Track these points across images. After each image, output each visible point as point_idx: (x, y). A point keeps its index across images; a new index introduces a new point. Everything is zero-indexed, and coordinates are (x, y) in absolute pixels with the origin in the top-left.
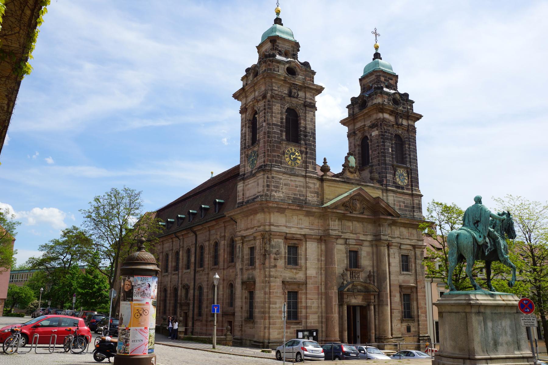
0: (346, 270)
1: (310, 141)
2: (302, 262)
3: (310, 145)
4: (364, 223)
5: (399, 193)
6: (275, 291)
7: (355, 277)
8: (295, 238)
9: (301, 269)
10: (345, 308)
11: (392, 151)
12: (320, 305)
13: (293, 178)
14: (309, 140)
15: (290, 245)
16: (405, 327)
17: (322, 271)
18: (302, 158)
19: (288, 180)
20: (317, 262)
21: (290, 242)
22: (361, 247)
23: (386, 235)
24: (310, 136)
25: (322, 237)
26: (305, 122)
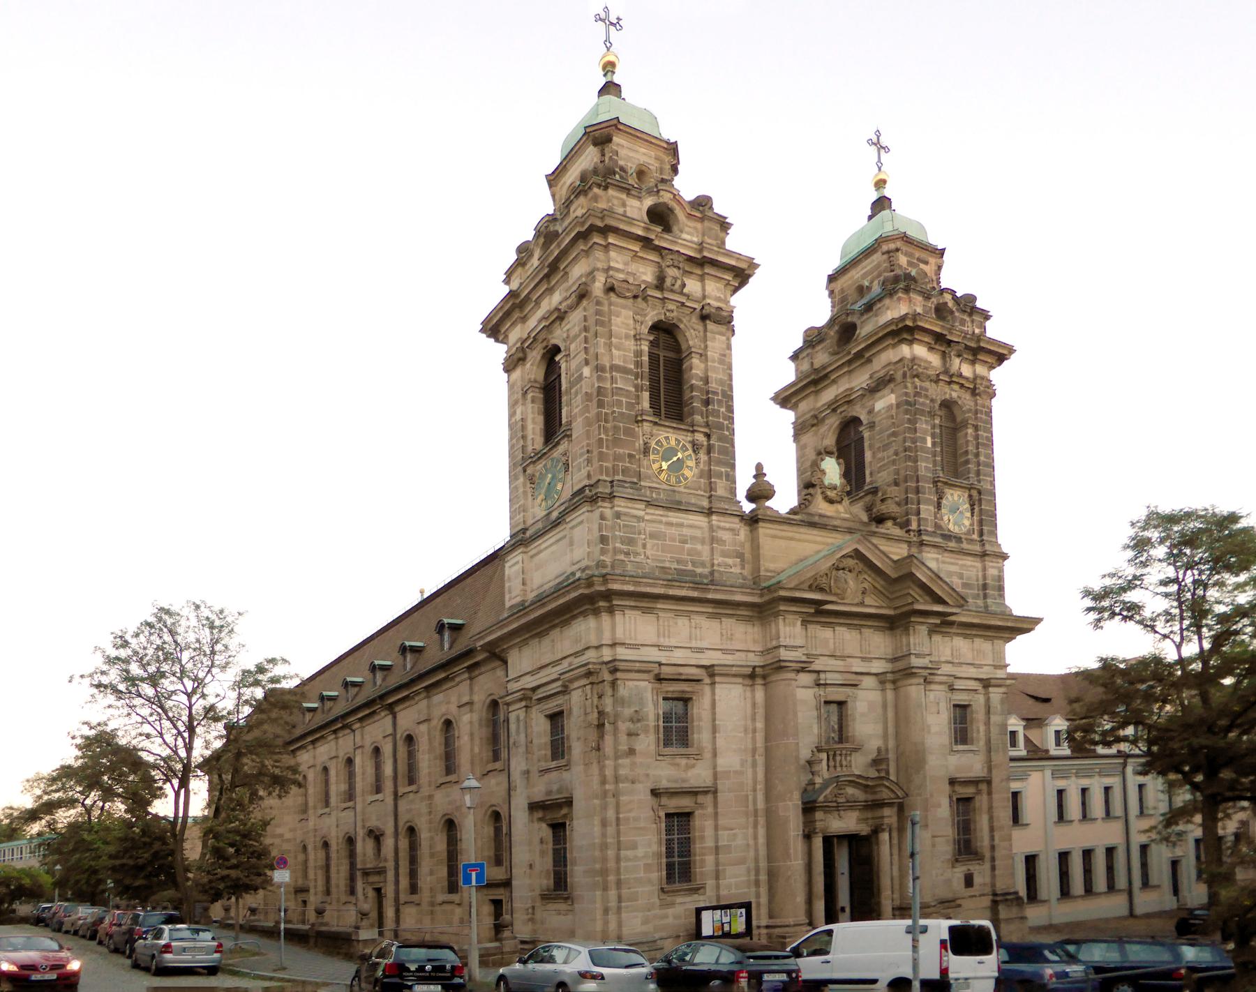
0: (819, 750)
1: (718, 416)
2: (701, 736)
3: (720, 427)
4: (863, 630)
6: (632, 815)
7: (841, 766)
8: (683, 677)
9: (698, 756)
10: (818, 843)
12: (751, 842)
13: (674, 517)
14: (716, 413)
15: (669, 695)
17: (757, 757)
18: (697, 463)
19: (661, 522)
20: (742, 735)
21: (671, 689)
22: (855, 691)
24: (720, 402)
25: (757, 669)
26: (702, 366)
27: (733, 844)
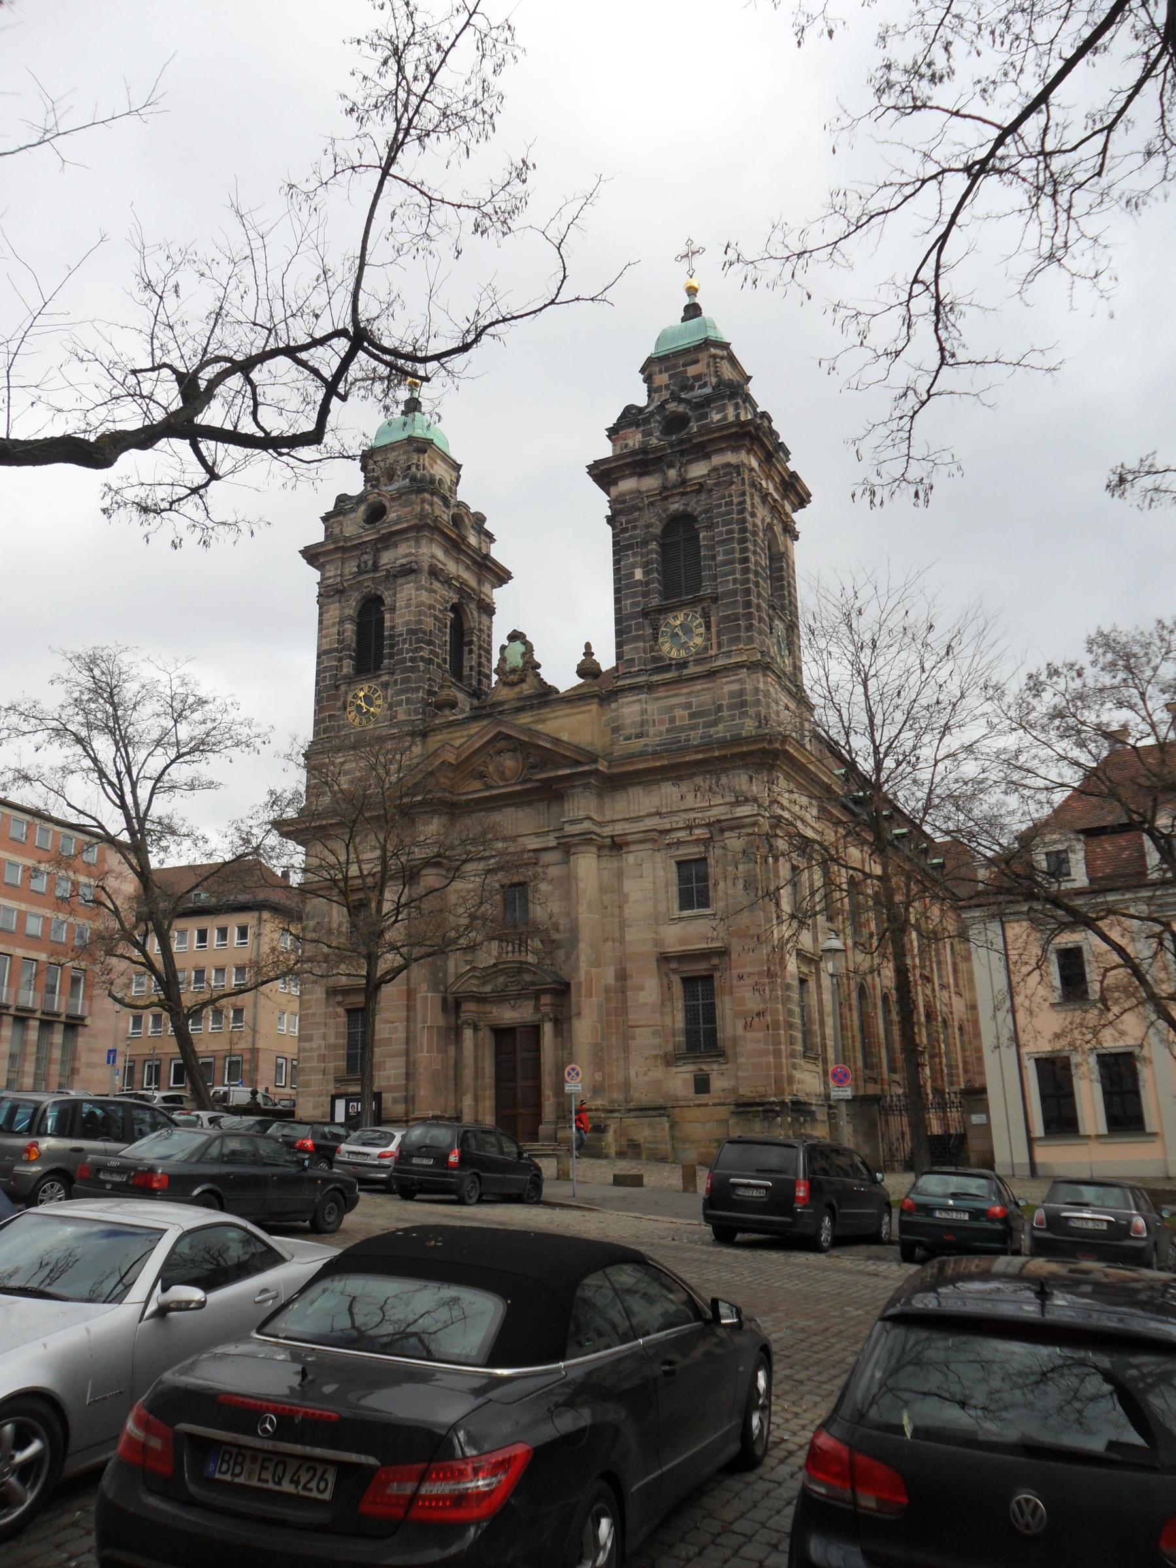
5: (664, 684)
11: (646, 573)
16: (690, 1077)
23: (580, 821)
27: (393, 1036)
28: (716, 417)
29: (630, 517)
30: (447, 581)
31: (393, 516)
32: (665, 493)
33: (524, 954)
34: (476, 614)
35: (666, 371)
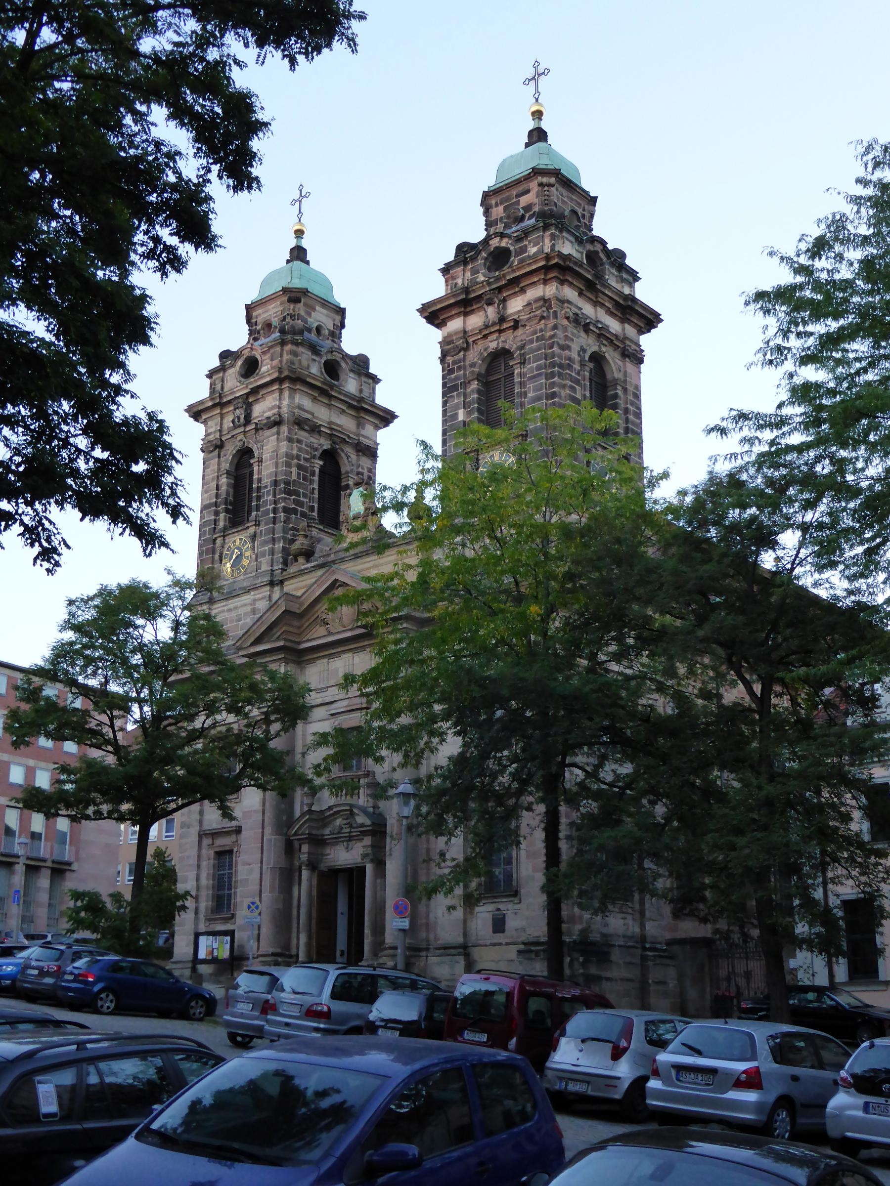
11: (469, 413)
16: (488, 917)
19: (223, 611)
28: (533, 250)
29: (456, 357)
30: (315, 429)
31: (264, 369)
32: (485, 332)
33: (355, 797)
34: (353, 457)
35: (501, 203)
